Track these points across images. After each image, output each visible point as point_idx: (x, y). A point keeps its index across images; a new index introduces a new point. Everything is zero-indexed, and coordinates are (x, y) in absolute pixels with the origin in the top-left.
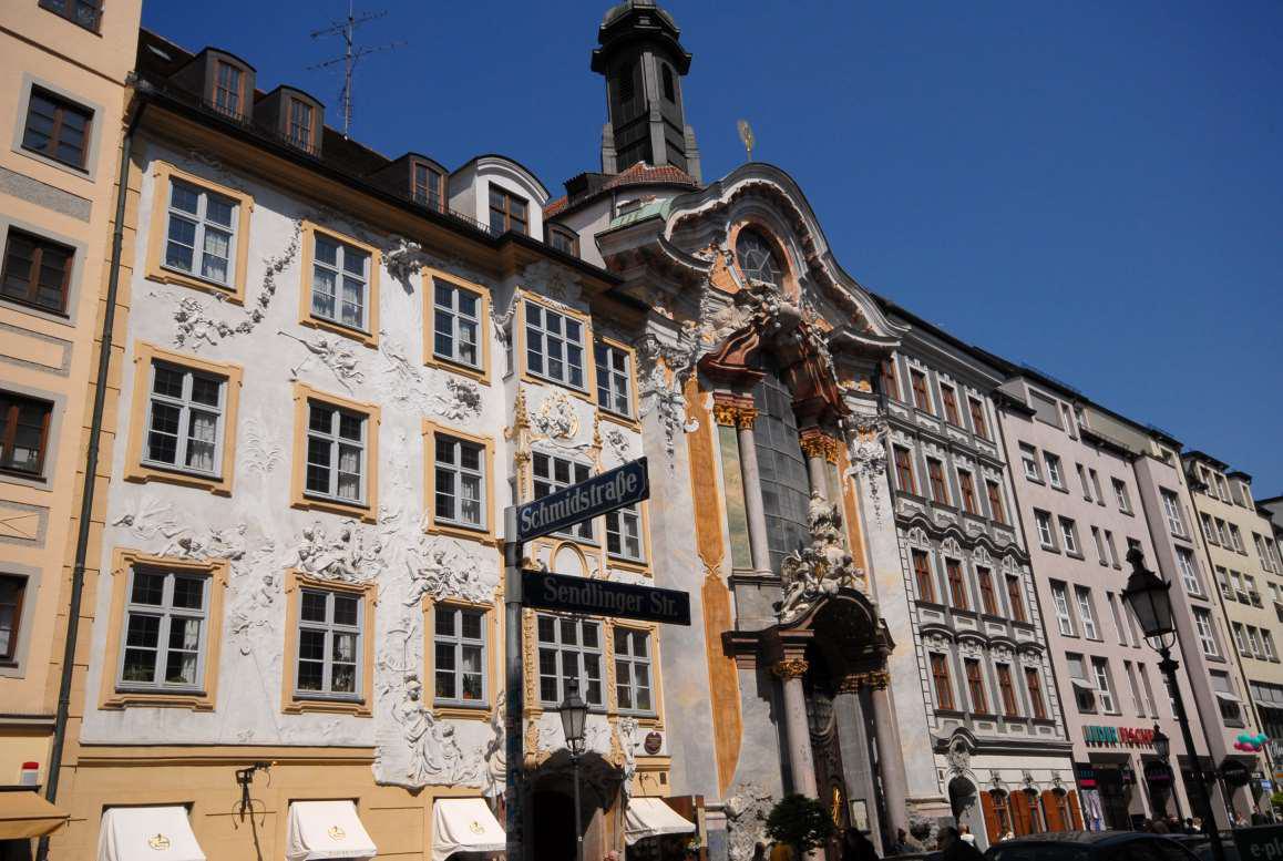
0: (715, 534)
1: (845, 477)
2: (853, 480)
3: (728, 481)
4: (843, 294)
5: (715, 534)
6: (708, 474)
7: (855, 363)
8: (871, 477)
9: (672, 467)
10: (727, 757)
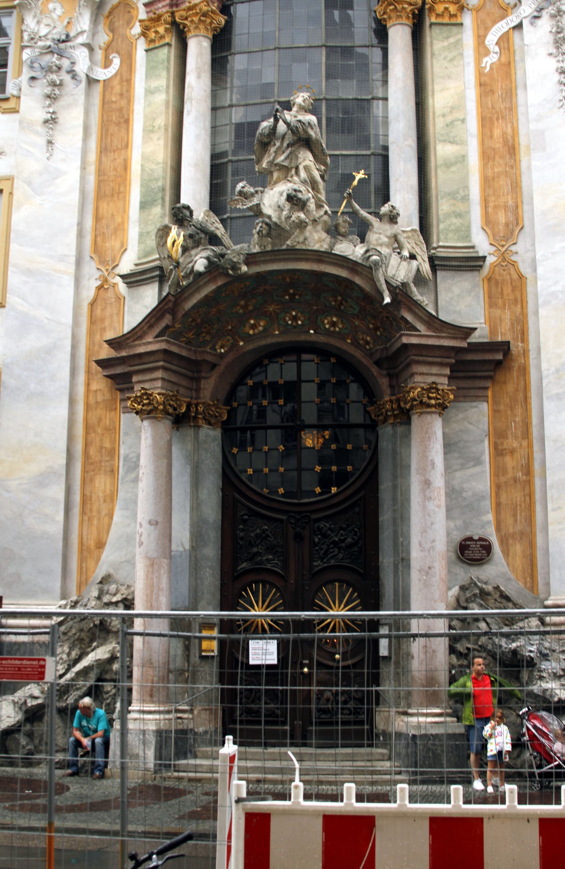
0: (119, 220)
1: (492, 39)
2: (516, 36)
3: (149, 131)
5: (119, 220)
6: (124, 131)
8: (553, 16)
9: (50, 142)
10: (92, 543)
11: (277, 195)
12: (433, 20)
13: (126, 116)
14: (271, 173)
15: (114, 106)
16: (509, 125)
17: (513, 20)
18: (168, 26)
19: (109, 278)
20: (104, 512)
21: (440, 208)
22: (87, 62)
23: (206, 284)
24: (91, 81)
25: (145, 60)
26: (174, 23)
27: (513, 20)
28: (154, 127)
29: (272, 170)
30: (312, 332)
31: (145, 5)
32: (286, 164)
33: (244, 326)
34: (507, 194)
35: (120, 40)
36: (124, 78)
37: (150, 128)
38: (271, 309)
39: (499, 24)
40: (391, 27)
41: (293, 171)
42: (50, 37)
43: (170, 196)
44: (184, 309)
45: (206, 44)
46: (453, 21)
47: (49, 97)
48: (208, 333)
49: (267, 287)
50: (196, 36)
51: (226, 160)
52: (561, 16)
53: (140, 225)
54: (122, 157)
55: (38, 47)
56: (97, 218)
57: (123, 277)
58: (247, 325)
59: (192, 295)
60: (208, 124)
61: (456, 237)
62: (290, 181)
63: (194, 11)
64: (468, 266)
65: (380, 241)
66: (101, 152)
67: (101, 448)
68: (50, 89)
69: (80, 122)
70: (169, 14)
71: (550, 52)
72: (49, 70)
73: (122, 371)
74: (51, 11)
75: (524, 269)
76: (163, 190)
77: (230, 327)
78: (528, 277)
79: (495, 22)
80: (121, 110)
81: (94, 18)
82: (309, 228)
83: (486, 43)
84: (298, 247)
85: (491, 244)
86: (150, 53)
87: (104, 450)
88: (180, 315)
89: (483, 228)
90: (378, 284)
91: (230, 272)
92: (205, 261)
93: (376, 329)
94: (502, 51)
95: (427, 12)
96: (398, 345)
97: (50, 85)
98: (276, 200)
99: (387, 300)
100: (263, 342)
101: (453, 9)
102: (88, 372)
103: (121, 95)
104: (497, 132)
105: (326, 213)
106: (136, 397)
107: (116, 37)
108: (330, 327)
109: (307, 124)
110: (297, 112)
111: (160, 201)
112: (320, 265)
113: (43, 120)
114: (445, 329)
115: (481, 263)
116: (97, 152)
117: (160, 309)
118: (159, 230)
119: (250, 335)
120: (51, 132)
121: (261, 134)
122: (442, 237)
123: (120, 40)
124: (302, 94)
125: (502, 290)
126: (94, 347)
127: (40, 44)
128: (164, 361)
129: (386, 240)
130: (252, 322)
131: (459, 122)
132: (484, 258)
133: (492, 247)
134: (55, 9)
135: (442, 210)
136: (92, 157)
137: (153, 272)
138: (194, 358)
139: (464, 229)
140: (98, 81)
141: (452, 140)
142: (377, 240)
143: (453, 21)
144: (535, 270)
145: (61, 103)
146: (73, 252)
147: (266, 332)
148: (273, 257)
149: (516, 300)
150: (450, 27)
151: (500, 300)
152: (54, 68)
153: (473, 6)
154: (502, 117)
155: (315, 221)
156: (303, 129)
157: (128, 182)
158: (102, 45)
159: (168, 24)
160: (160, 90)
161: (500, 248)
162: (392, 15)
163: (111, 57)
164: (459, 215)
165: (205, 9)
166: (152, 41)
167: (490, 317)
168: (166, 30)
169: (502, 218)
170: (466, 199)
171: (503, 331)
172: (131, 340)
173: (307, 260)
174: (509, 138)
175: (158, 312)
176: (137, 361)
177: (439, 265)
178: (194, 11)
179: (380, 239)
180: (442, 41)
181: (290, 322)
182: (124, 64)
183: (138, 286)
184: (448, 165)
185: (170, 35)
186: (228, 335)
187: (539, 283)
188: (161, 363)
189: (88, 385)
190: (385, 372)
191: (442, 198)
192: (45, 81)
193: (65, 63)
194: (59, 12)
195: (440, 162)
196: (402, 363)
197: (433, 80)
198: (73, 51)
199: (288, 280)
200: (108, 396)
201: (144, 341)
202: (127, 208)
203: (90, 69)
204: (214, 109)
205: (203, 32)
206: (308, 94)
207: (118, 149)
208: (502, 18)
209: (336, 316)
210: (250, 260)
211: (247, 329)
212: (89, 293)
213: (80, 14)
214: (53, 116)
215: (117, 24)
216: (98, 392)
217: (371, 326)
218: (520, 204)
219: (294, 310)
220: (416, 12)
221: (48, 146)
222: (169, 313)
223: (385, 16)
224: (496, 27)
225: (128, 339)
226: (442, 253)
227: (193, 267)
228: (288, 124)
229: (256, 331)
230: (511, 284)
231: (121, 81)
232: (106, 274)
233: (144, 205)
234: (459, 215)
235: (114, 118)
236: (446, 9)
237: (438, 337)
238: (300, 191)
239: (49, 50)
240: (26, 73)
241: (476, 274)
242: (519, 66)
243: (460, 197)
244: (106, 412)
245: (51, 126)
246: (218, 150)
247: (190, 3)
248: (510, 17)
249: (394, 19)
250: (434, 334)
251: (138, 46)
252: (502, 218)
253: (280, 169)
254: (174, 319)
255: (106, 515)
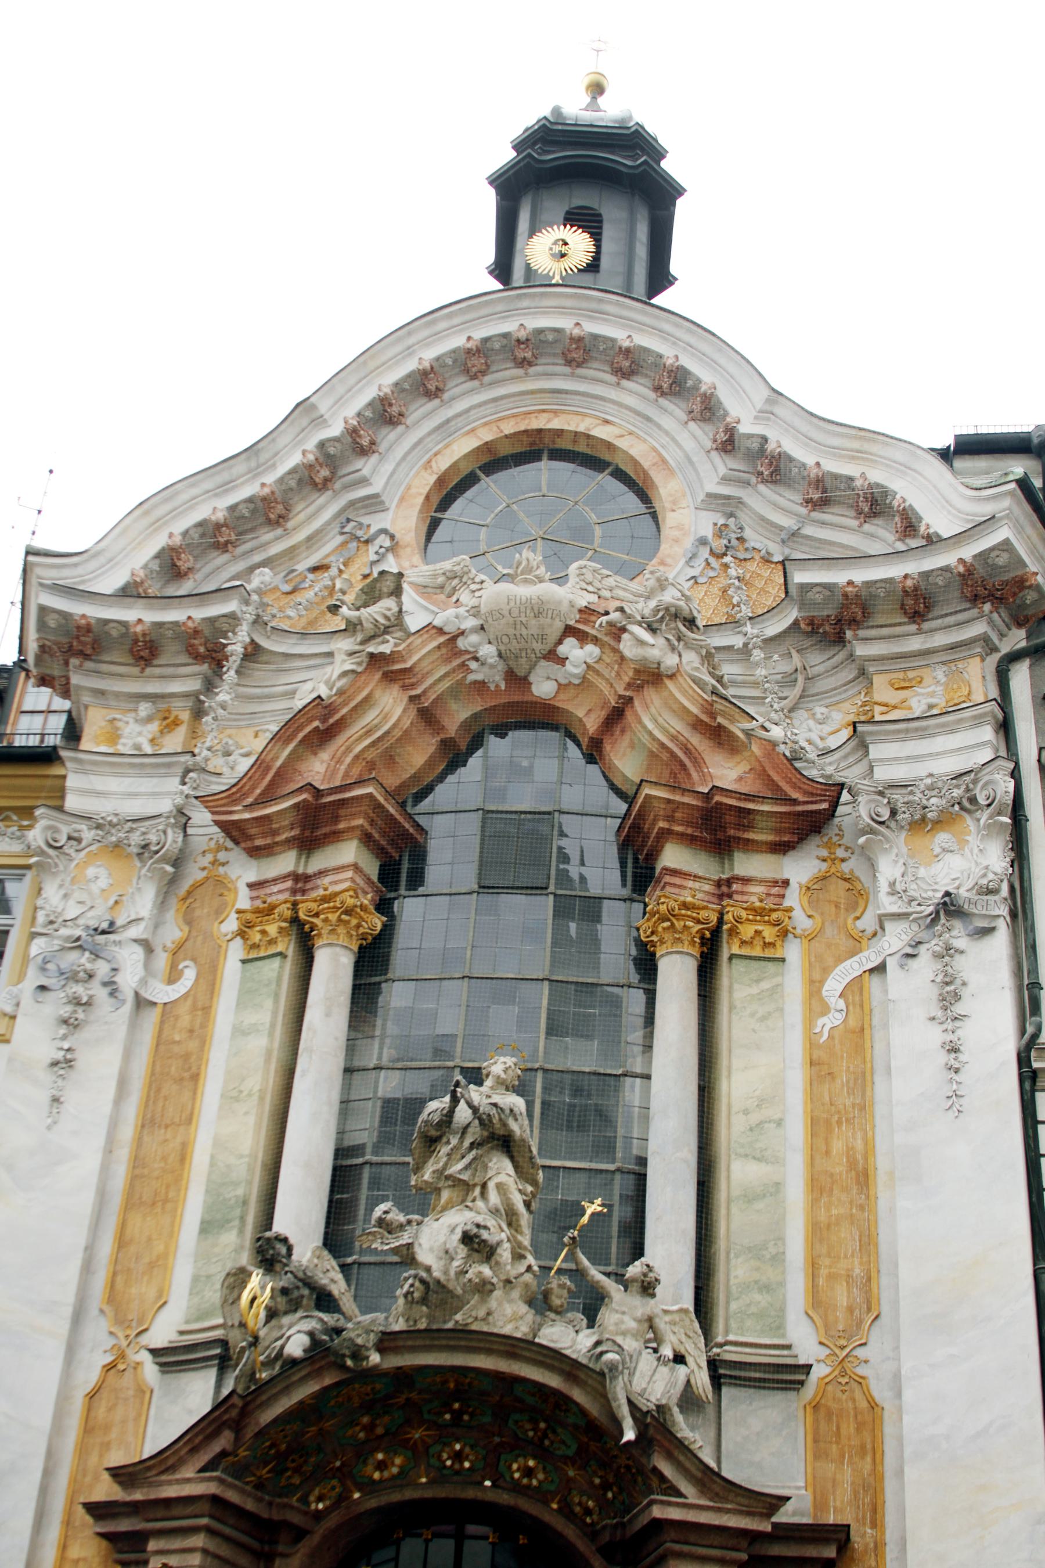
0: (159, 1248)
1: (833, 986)
3: (231, 1097)
4: (851, 479)
5: (159, 1248)
7: (915, 644)
11: (445, 1231)
12: (736, 950)
13: (194, 1069)
14: (438, 1191)
15: (176, 1049)
16: (859, 1135)
17: (869, 958)
18: (284, 925)
19: (129, 1352)
21: (733, 1274)
22: (140, 971)
23: (303, 1380)
24: (141, 1003)
25: (238, 976)
26: (295, 920)
27: (869, 958)
28: (241, 1092)
29: (440, 1185)
30: (488, 1483)
31: (251, 886)
32: (465, 1177)
33: (365, 1462)
34: (853, 1256)
35: (200, 938)
36: (200, 1004)
37: (234, 1094)
38: (417, 1436)
39: (848, 963)
40: (662, 956)
41: (477, 1191)
42: (81, 922)
43: (256, 1217)
44: (257, 1423)
45: (346, 961)
46: (769, 953)
47: (65, 1022)
48: (297, 1470)
49: (413, 1395)
50: (330, 945)
51: (360, 1160)
52: (951, 956)
53: (195, 1262)
54: (179, 1140)
55: (59, 937)
56: (122, 1242)
57: (155, 1352)
58: (371, 1461)
59: (275, 1398)
60: (335, 1096)
61: (758, 1327)
62: (471, 1209)
63: (332, 904)
64: (778, 1381)
65: (623, 1327)
66: (143, 1126)
68: (69, 1008)
69: (114, 1070)
70: (289, 905)
71: (932, 1015)
72: (72, 977)
74: (90, 881)
75: (880, 1392)
76: (245, 1203)
77: (338, 1464)
78: (886, 1406)
79: (840, 960)
80: (186, 1057)
81: (161, 899)
82: (497, 1293)
83: (824, 993)
84: (474, 1327)
85: (821, 1343)
86: (248, 966)
88: (250, 1432)
89: (807, 1313)
90: (614, 1404)
91: (349, 1363)
92: (305, 1340)
93: (606, 1486)
94: (851, 1008)
95: (725, 936)
96: (643, 1520)
97: (70, 1002)
98: (442, 1239)
99: (629, 1435)
100: (396, 1497)
101: (769, 933)
102: (68, 1523)
103: (191, 1031)
104: (838, 1146)
105: (529, 1268)
107: (194, 933)
108: (523, 1476)
109: (508, 1112)
110: (492, 1088)
111: (236, 1223)
112: (511, 1362)
113: (49, 1061)
114: (731, 1496)
115: (802, 1377)
116: (136, 1126)
117: (214, 1420)
118: (228, 1274)
119: (374, 1481)
120: (60, 1083)
121: (426, 1122)
122: (733, 1324)
123: (200, 938)
124: (502, 1059)
125: (838, 1428)
126: (84, 1476)
127: (64, 932)
128: (211, 1516)
129: (633, 1325)
130: (380, 1456)
131: (773, 1125)
132: (807, 1368)
133: (823, 1348)
134: (97, 878)
135: (736, 1277)
136: (127, 1132)
137: (209, 1349)
138: (265, 1515)
139: (773, 1313)
140: (155, 1004)
141: (758, 1155)
142: (616, 1324)
143: (769, 953)
144: (899, 1395)
145: (86, 1034)
146: (69, 1297)
147: (403, 1478)
148: (428, 1342)
149: (863, 1447)
150: (762, 963)
151: (834, 1446)
152: (82, 974)
153: (804, 930)
154: (847, 1120)
155: (508, 1282)
156: (500, 1119)
157: (184, 1182)
158: (169, 945)
159: (285, 921)
160: (258, 1031)
161: (837, 1351)
162: (667, 936)
163: (181, 967)
164: (766, 1288)
165: (350, 902)
166: (255, 946)
167: (814, 1477)
168: (281, 930)
169: (841, 1296)
170: (778, 1259)
171: (838, 1504)
172: (154, 1472)
173: (489, 1352)
174: (859, 1157)
175: (210, 1424)
176: (160, 1513)
177: (726, 1376)
178: (332, 904)
179: (622, 1322)
180: (749, 986)
181: (449, 1463)
182: (201, 981)
183: (180, 1371)
184: (750, 1197)
185: (286, 939)
186: (334, 1477)
187: (906, 1419)
188: (204, 1521)
189: (64, 1547)
191: (737, 1257)
192: (63, 995)
193: (102, 969)
194: (103, 882)
195: (735, 1192)
196: (649, 1555)
197: (730, 1051)
198: (116, 949)
199: (452, 1385)
201: (178, 1476)
202: (176, 1229)
203: (144, 982)
204: (349, 1071)
205: (343, 940)
206: (514, 1059)
207: (173, 1123)
208: (853, 953)
209: (534, 1458)
210: (386, 1344)
211: (369, 1468)
212: (89, 1375)
213: (139, 889)
214: (69, 1056)
215: (198, 913)
216: (81, 1564)
217: (597, 1481)
218: (874, 1274)
219: (458, 1441)
220: (708, 934)
221: (51, 1106)
222: (230, 1428)
223: (654, 938)
224: (841, 967)
225: (149, 1468)
226: (731, 1354)
227: (282, 1347)
228: (475, 1109)
229: (386, 1474)
230: (856, 1416)
231: (194, 1008)
232: (124, 1343)
233: (207, 1227)
234: (766, 1288)
235: (173, 1069)
236: (758, 933)
237: (719, 1510)
238: (486, 1228)
239: (77, 944)
240: (33, 978)
241: (792, 1395)
242: (878, 1035)
243: (768, 1256)
245: (62, 1072)
246: (351, 1140)
247: (326, 889)
248: (865, 953)
249: (669, 944)
250: (711, 1504)
251: (230, 953)
252: (841, 1296)
253: (454, 1186)
254: (237, 1439)
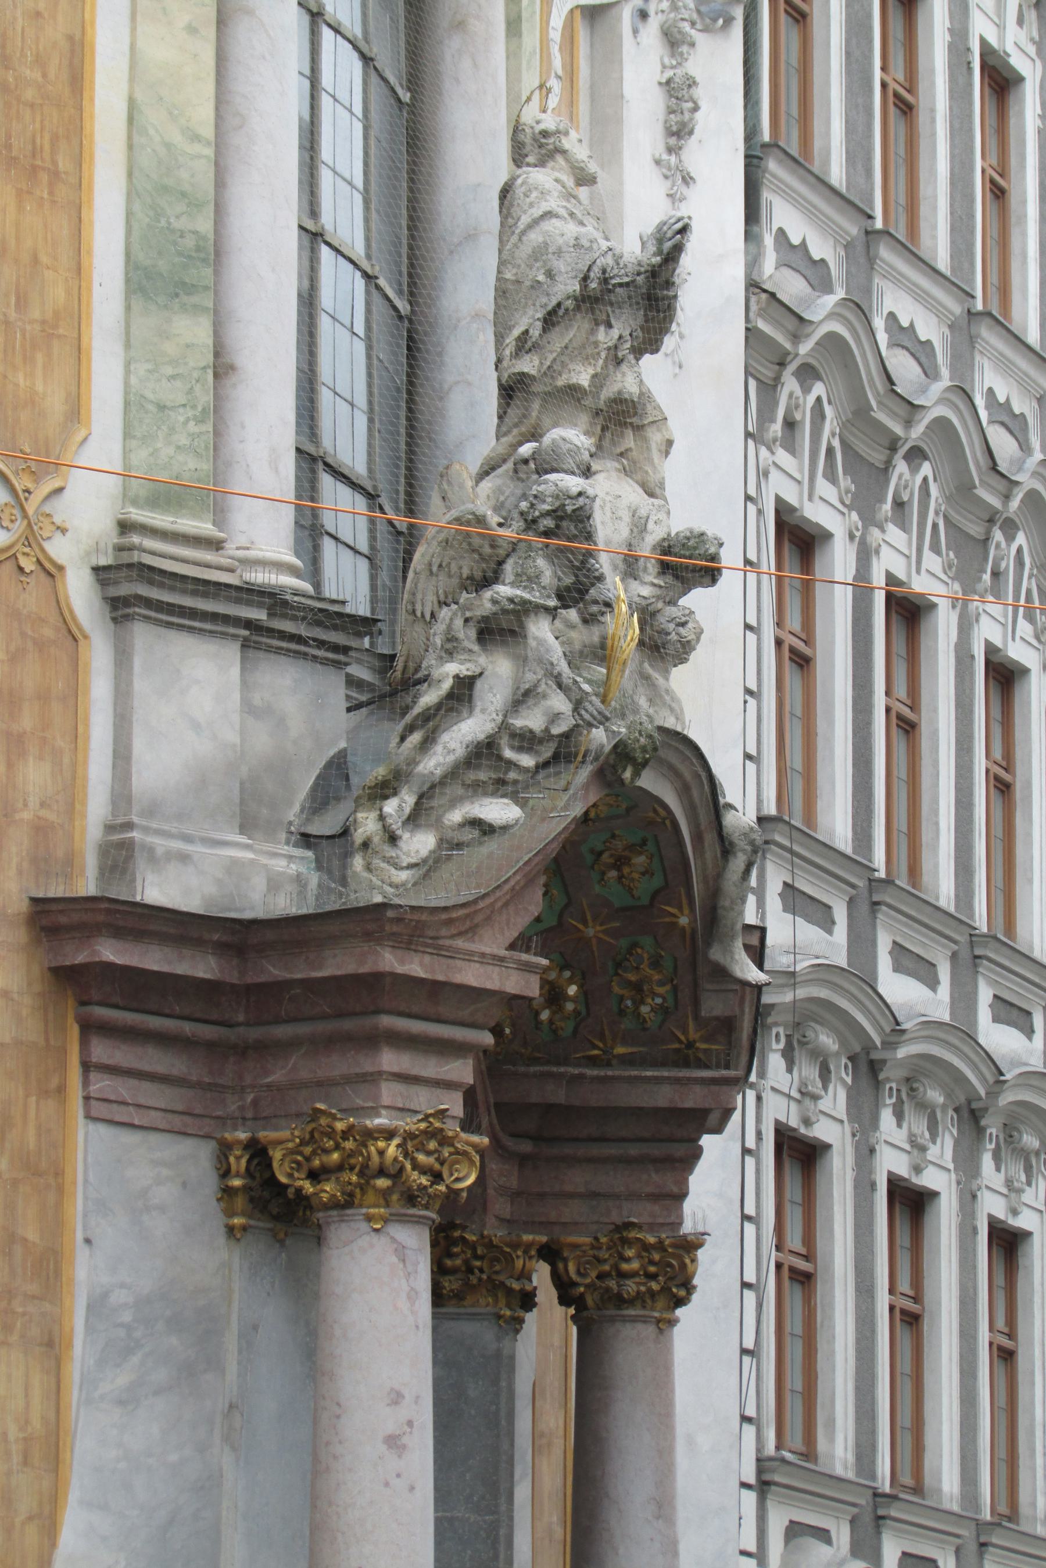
0: (57, 294)
20: (25, 1505)
67: (12, 1238)
73: (166, 969)
87: (18, 1250)
106: (409, 1136)
183: (169, 625)
190: (526, 1147)
200: (32, 1031)
225: (450, 922)
244: (27, 1096)
255: (30, 1518)
